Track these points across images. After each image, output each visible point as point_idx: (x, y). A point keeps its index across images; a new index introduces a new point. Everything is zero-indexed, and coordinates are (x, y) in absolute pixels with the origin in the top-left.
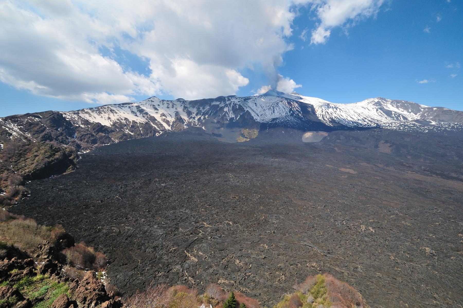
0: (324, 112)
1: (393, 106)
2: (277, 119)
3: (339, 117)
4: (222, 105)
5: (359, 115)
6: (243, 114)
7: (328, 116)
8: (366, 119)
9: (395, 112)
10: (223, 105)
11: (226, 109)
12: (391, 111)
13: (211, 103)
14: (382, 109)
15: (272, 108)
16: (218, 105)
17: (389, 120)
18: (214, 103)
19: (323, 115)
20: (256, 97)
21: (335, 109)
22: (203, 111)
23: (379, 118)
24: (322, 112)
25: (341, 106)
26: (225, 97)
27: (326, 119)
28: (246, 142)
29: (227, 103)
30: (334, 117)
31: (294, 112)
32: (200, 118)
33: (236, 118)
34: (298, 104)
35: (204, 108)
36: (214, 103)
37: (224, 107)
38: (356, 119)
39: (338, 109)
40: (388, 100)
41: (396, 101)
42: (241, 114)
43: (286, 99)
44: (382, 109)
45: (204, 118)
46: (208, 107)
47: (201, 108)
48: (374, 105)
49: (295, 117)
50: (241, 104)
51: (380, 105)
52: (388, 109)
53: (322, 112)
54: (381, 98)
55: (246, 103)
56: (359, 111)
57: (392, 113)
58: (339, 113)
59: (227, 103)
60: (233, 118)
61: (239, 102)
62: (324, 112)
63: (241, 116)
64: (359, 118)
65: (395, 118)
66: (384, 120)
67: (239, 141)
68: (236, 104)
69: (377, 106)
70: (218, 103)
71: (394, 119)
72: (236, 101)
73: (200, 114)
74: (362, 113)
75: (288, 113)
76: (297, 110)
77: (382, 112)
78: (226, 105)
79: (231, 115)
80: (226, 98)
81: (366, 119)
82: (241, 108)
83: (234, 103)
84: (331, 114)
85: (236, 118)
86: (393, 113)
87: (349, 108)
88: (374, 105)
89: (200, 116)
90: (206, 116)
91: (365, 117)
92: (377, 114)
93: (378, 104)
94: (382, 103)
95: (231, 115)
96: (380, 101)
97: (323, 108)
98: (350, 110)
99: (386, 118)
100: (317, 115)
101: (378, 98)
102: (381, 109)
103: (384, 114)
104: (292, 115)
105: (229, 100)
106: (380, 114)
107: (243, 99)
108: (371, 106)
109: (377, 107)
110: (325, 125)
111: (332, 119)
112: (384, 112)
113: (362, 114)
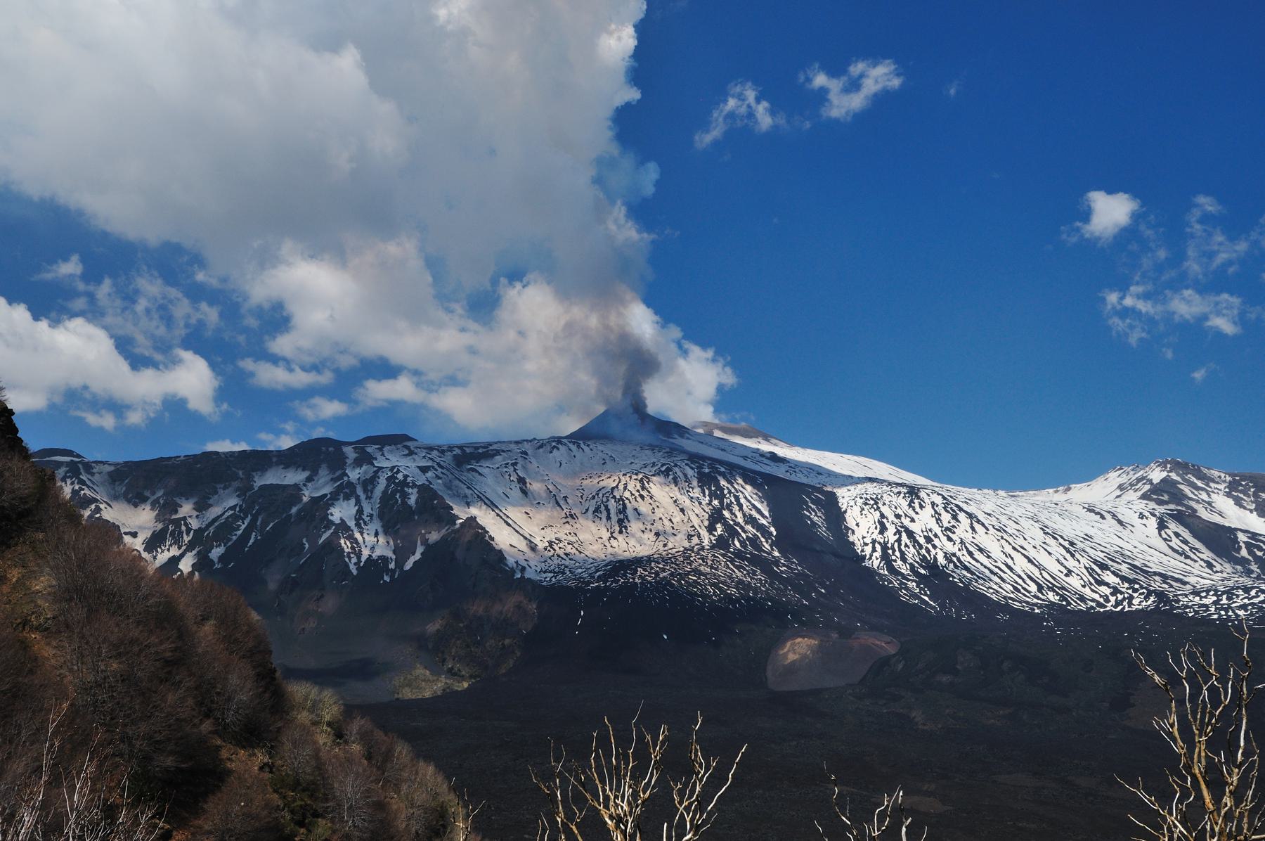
0: (891, 530)
1: (1238, 502)
2: (638, 562)
3: (966, 559)
4: (323, 486)
5: (1071, 548)
6: (443, 539)
7: (911, 552)
8: (1104, 567)
9: (1254, 536)
10: (327, 490)
11: (341, 512)
12: (1232, 531)
13: (250, 478)
14: (1186, 518)
15: (612, 504)
16: (297, 487)
17: (1225, 574)
18: (272, 478)
19: (884, 547)
20: (526, 447)
21: (946, 518)
22: (195, 524)
23: (1175, 565)
24: (883, 529)
25: (984, 501)
26: (338, 445)
27: (905, 569)
28: (448, 695)
29: (354, 474)
30: (941, 560)
31: (731, 531)
32: (175, 561)
33: (400, 564)
34: (754, 485)
35: (201, 507)
36: (272, 478)
37: (334, 498)
38: (1054, 568)
39: (962, 516)
40: (1215, 473)
41: (1251, 478)
42: (434, 537)
43: (694, 458)
44: (1186, 518)
45: (203, 564)
46: (233, 501)
47: (186, 509)
48: (1144, 497)
49: (739, 555)
50: (438, 485)
51: (1178, 497)
52: (1217, 519)
53: (883, 529)
54: (1178, 466)
55: (466, 476)
56: (1069, 529)
57: (1236, 540)
58: (968, 537)
59: (354, 474)
60: (384, 559)
61: (424, 470)
62: (891, 530)
63: (429, 548)
64: (1071, 563)
65: (1254, 567)
66: (1200, 579)
67: (408, 694)
68: (404, 483)
69: (1161, 503)
70: (293, 477)
71: (1248, 572)
72: (408, 466)
73: (177, 541)
74: (1088, 537)
75: (704, 533)
76: (751, 520)
77: (1186, 534)
78: (346, 491)
79: (373, 543)
80: (350, 452)
81: (1104, 567)
82: (433, 508)
83: (391, 479)
84: (928, 540)
85: (400, 564)
86: (1242, 537)
87: (1018, 512)
88: (1144, 497)
89: (175, 551)
90: (216, 553)
91: (1100, 556)
92: (1162, 546)
93: (1162, 492)
94: (1187, 490)
95: (373, 543)
96: (1174, 476)
97: (885, 510)
98: (1026, 524)
99: (1210, 566)
100: (858, 549)
101: (1163, 465)
102: (1179, 518)
103: (1198, 545)
104: (722, 543)
105: (364, 458)
106: (1175, 543)
107: (448, 457)
108: (1132, 505)
109: (1161, 510)
110: (892, 594)
111: (932, 566)
112: (1195, 536)
113: (1086, 545)
